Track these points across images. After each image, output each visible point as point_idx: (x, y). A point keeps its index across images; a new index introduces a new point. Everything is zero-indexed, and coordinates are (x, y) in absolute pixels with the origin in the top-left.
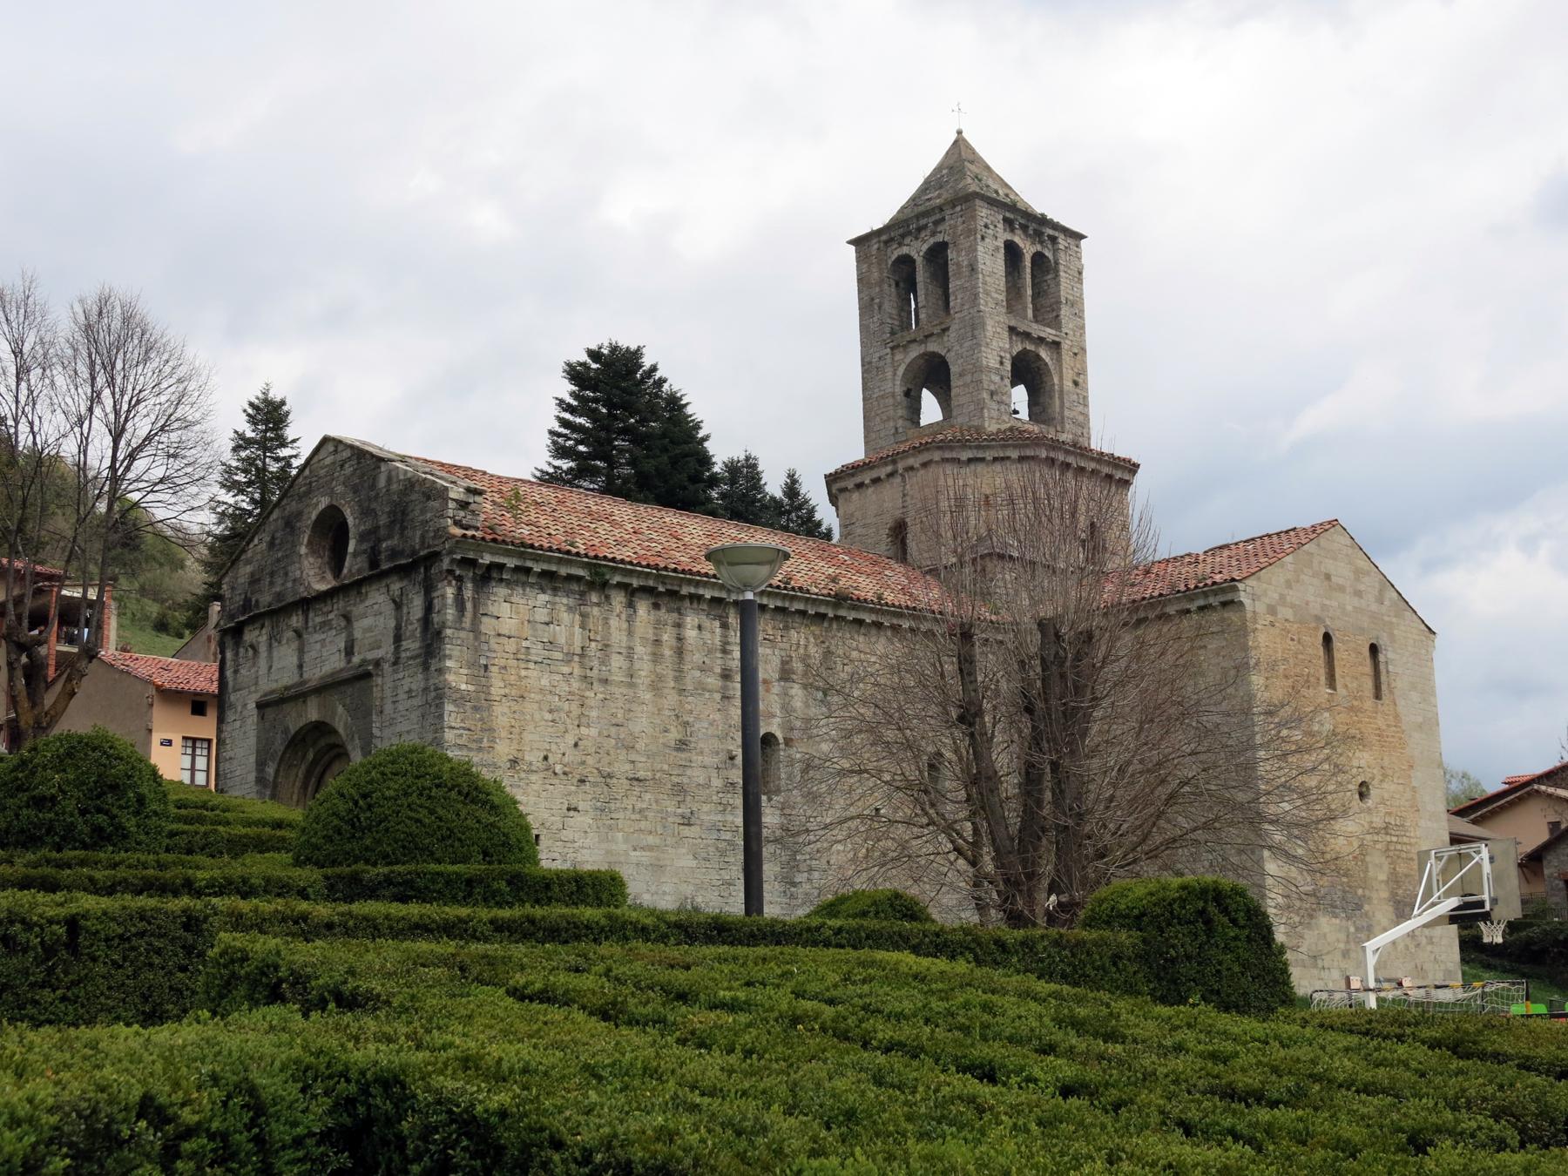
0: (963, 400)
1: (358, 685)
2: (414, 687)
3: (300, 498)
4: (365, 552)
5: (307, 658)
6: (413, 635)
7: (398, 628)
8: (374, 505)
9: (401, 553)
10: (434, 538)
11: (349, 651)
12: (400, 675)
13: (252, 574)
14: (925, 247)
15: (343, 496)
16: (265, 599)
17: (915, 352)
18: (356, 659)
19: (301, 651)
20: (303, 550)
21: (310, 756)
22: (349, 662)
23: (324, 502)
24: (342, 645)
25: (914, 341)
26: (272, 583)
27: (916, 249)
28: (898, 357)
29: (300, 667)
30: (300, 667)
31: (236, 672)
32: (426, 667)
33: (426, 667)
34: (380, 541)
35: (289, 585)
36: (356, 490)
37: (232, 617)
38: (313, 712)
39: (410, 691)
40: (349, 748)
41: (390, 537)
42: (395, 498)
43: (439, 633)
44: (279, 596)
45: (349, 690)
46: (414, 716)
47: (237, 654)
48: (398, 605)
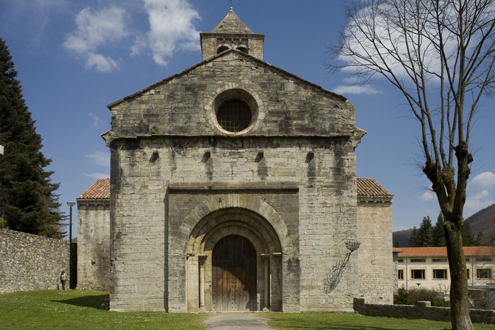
1: (281, 195)
2: (327, 201)
4: (276, 122)
5: (216, 169)
6: (326, 174)
8: (283, 98)
9: (312, 130)
10: (343, 128)
11: (263, 171)
12: (316, 194)
13: (148, 110)
15: (250, 86)
16: (165, 128)
18: (273, 179)
20: (208, 108)
21: (214, 223)
23: (230, 86)
24: (256, 168)
26: (172, 120)
29: (210, 174)
30: (210, 174)
31: (132, 165)
32: (339, 193)
33: (339, 193)
34: (288, 118)
35: (194, 125)
36: (263, 86)
37: (127, 132)
38: (234, 201)
40: (274, 226)
41: (302, 119)
42: (305, 99)
43: (349, 178)
44: (181, 129)
45: (274, 195)
46: (329, 217)
47: (133, 155)
48: (310, 157)
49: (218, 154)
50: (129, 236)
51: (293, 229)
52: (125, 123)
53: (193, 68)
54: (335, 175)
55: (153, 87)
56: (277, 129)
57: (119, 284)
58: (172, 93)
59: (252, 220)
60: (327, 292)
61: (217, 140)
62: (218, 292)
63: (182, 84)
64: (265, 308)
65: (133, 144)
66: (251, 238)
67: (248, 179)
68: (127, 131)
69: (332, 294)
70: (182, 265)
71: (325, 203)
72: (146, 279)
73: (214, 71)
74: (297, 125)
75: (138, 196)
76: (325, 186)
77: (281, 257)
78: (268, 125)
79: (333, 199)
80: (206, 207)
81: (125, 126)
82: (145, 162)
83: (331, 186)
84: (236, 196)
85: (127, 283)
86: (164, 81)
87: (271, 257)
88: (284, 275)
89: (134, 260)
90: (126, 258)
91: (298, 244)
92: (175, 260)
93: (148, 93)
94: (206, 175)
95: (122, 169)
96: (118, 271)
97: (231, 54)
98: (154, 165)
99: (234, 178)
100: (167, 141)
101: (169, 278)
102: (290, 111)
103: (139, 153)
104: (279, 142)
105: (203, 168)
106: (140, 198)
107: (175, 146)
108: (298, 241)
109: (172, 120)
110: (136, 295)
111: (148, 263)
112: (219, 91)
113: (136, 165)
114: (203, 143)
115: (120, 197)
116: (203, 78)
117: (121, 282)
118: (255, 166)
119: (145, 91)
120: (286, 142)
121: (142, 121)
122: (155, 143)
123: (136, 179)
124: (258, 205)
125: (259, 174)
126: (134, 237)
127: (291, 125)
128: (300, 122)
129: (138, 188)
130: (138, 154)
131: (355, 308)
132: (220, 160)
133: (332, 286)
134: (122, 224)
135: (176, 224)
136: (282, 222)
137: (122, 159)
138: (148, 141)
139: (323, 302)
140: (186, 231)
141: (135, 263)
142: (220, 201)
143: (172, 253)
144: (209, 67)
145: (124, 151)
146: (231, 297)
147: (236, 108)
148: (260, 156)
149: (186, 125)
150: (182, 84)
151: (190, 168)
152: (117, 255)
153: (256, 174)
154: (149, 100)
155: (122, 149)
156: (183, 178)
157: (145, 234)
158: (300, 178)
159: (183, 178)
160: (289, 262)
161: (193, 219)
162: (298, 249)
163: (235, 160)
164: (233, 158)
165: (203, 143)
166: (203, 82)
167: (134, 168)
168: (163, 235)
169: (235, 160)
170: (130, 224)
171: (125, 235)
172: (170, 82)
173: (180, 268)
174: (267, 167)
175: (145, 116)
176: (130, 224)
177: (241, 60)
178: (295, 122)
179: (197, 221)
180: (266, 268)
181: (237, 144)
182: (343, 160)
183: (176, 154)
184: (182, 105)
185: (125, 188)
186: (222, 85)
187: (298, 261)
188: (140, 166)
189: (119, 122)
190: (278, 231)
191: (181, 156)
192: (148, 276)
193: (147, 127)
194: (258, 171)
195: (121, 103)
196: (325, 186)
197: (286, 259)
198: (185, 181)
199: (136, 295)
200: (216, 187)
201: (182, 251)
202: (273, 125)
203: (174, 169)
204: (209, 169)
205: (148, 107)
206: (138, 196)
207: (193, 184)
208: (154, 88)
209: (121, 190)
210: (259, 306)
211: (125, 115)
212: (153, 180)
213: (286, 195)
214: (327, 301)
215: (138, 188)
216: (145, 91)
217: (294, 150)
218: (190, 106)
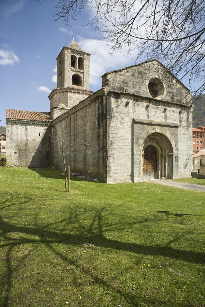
0: (85, 85)
2: (185, 132)
3: (145, 69)
4: (170, 96)
5: (150, 114)
7: (180, 118)
12: (182, 129)
14: (79, 57)
16: (131, 91)
17: (75, 73)
18: (170, 122)
19: (148, 112)
22: (166, 121)
24: (164, 116)
25: (76, 71)
26: (134, 87)
27: (78, 57)
28: (72, 72)
29: (148, 116)
30: (148, 116)
31: (117, 107)
35: (142, 91)
37: (114, 89)
38: (158, 130)
39: (184, 133)
40: (171, 142)
41: (177, 96)
45: (171, 128)
47: (117, 101)
49: (151, 107)
50: (116, 144)
51: (177, 143)
52: (114, 84)
53: (142, 64)
54: (187, 122)
55: (126, 68)
56: (170, 100)
57: (111, 169)
58: (133, 74)
59: (161, 139)
60: (184, 169)
61: (151, 101)
62: (145, 171)
63: (137, 70)
64: (163, 178)
65: (117, 96)
66: (157, 146)
67: (161, 120)
68: (115, 88)
69: (185, 170)
70: (139, 159)
71: (184, 133)
72: (123, 166)
73: (149, 67)
74: (176, 99)
75: (120, 124)
76: (184, 126)
77: (173, 155)
78: (167, 97)
79: (186, 132)
80: (149, 132)
81: (114, 85)
82: (122, 106)
83: (186, 126)
84: (159, 127)
85: (116, 168)
86: (131, 66)
87: (167, 155)
88: (174, 163)
89: (118, 157)
90: (115, 156)
91: (178, 150)
92: (137, 157)
93: (123, 71)
94: (147, 116)
95: (112, 108)
96: (111, 162)
97: (155, 61)
98: (126, 108)
99: (157, 119)
100: (132, 97)
101: (134, 166)
102: (174, 93)
103: (120, 101)
104: (171, 106)
105: (145, 112)
106: (121, 125)
107: (135, 100)
108: (178, 148)
109: (134, 87)
110: (119, 175)
111: (124, 158)
112: (151, 77)
113: (118, 107)
114: (145, 101)
115: (112, 123)
116: (145, 69)
117: (112, 168)
118: (163, 115)
119: (123, 69)
120: (173, 106)
121: (121, 85)
122: (126, 97)
123: (119, 114)
124: (166, 133)
125: (165, 118)
126: (118, 144)
127: (174, 99)
128: (177, 98)
129: (120, 119)
130: (119, 101)
131: (192, 176)
132: (151, 110)
133: (186, 167)
134: (113, 137)
135: (137, 139)
136: (173, 140)
137: (113, 103)
138: (123, 96)
139: (183, 174)
140: (141, 142)
141: (119, 158)
142: (153, 129)
143: (135, 153)
144: (147, 65)
145: (114, 99)
146: (148, 173)
147: (155, 86)
148: (165, 110)
149: (139, 91)
150: (137, 70)
151: (140, 111)
152: (111, 154)
153: (164, 118)
154: (124, 74)
155: (112, 98)
156: (138, 116)
157: (123, 143)
158: (177, 122)
159: (138, 116)
160: (175, 157)
161: (144, 137)
162: (178, 152)
163: (157, 111)
164: (156, 110)
165: (147, 101)
166: (145, 72)
167: (118, 108)
168: (130, 144)
169: (157, 111)
170: (116, 137)
171: (114, 143)
172: (133, 68)
173: (139, 161)
174: (167, 116)
175: (122, 82)
176: (116, 137)
177: (158, 65)
178: (175, 97)
179: (145, 138)
180: (163, 160)
181: (157, 104)
182: (189, 116)
183: (135, 104)
184: (137, 81)
185: (114, 119)
186: (152, 75)
187: (178, 157)
188: (120, 108)
189: (111, 83)
190: (172, 145)
191: (137, 106)
192: (124, 164)
193: (123, 88)
194: (165, 117)
195: (112, 73)
196: (184, 126)
197: (174, 156)
198: (139, 118)
199: (119, 175)
200: (152, 123)
201: (139, 152)
202: (169, 97)
203: (135, 111)
204: (148, 114)
205: (124, 78)
206: (120, 124)
207: (143, 120)
208: (126, 69)
209: (112, 119)
210: (159, 176)
211: (114, 80)
212: (126, 116)
213: (174, 129)
214: (184, 173)
215: (120, 119)
216: (123, 69)
217: (175, 109)
218: (141, 82)
